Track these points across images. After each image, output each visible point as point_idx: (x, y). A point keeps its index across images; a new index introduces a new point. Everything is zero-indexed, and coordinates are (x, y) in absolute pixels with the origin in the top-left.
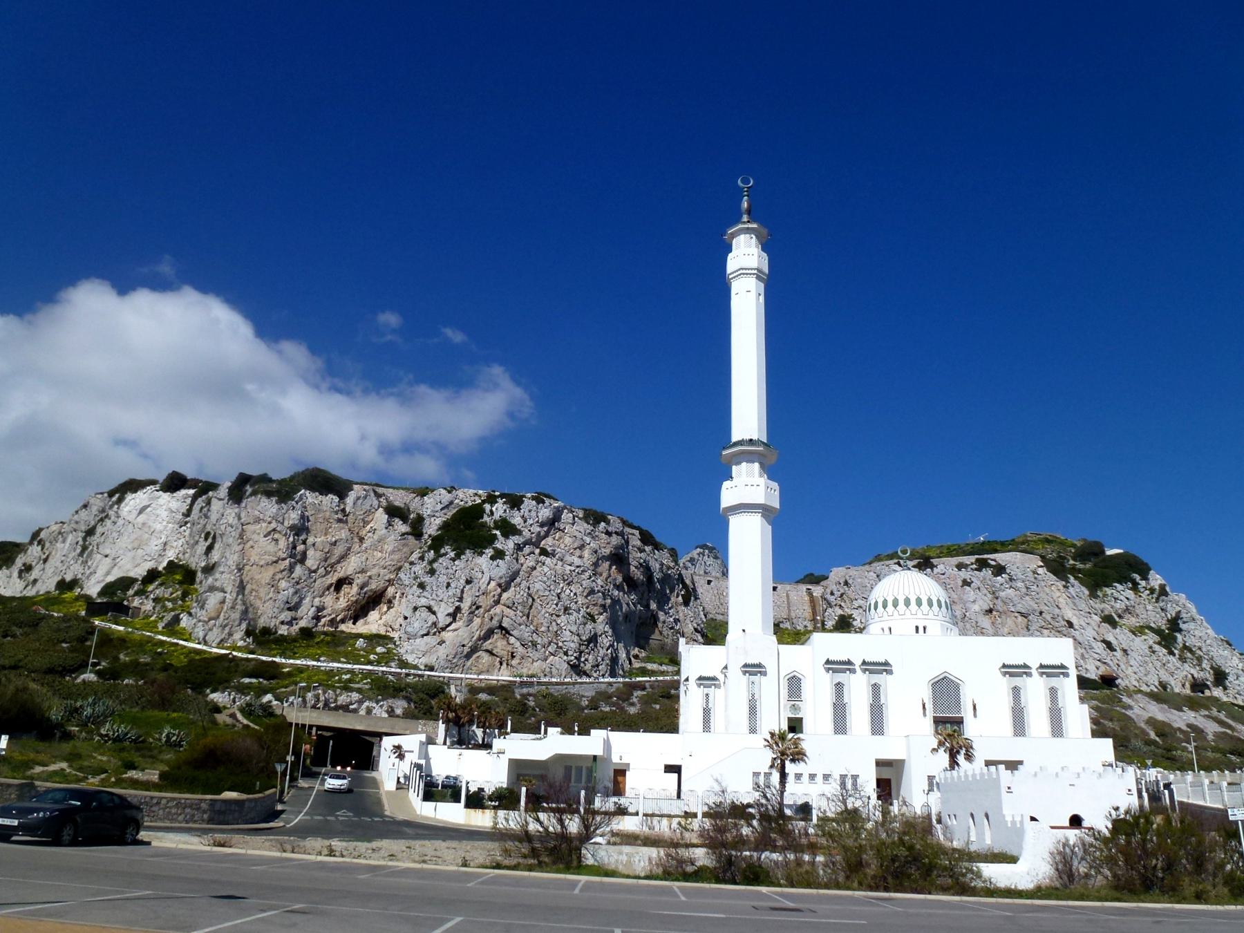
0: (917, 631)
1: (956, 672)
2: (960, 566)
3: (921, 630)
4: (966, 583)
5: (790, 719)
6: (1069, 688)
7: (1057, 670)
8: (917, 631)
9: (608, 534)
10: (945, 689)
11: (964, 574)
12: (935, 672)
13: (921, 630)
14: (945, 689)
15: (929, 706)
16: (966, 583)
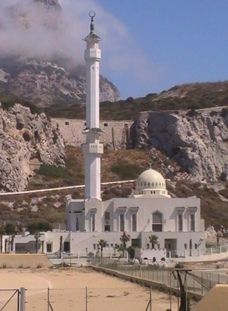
0: (152, 193)
1: (160, 210)
2: (213, 114)
3: (153, 192)
4: (215, 124)
5: (105, 226)
6: (197, 215)
7: (192, 211)
8: (152, 193)
9: (14, 113)
10: (158, 215)
11: (214, 119)
12: (154, 210)
13: (153, 192)
14: (158, 215)
15: (151, 221)
16: (215, 124)
